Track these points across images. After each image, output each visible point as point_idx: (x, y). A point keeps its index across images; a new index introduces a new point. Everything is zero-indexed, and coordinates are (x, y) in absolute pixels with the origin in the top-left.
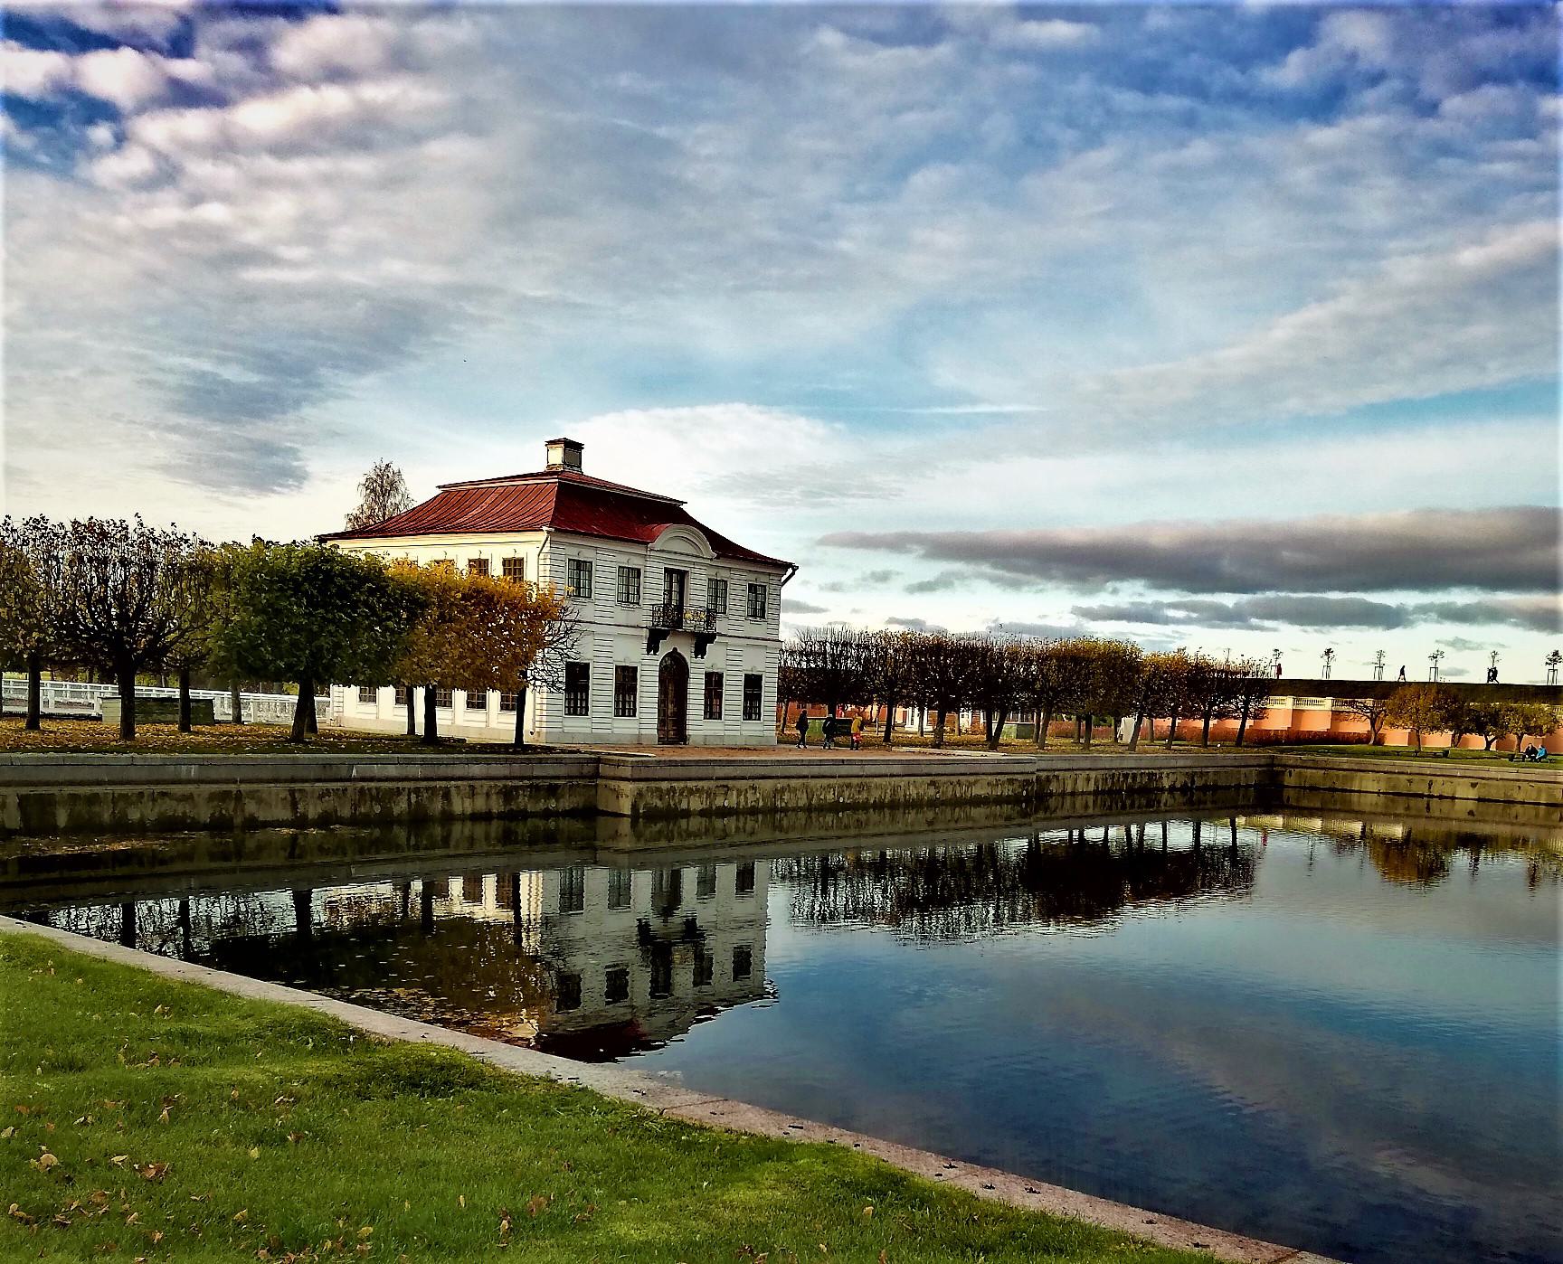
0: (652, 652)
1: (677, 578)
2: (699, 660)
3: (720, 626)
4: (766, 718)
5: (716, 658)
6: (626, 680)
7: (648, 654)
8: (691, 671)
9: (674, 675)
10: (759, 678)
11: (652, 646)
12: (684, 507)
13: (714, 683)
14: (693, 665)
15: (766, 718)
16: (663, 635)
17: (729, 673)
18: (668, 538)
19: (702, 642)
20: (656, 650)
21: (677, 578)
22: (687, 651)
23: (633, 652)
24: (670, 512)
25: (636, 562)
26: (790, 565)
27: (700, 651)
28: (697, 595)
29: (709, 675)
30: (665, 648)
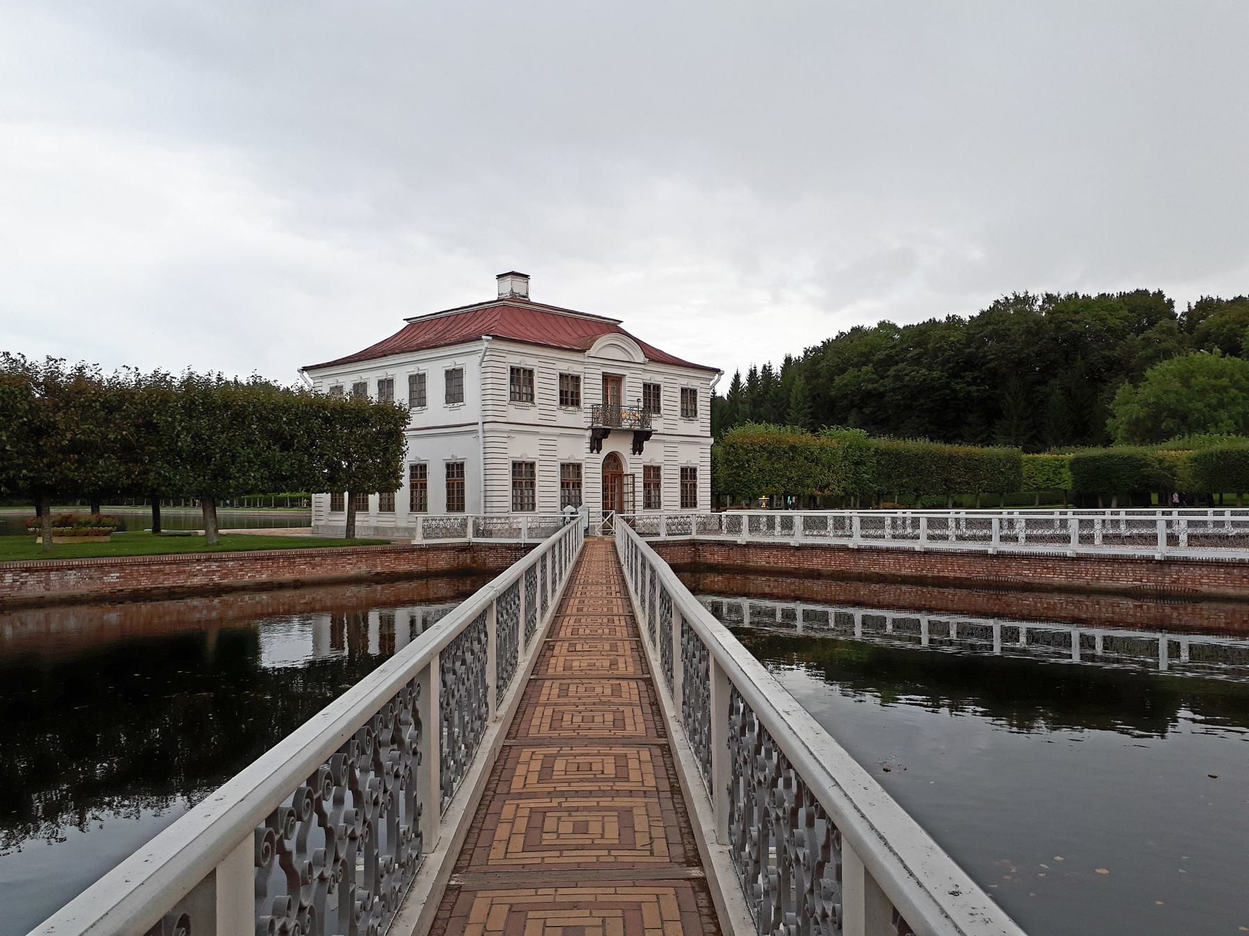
0: (595, 451)
1: (612, 382)
2: (637, 456)
3: (656, 424)
4: (666, 508)
5: (653, 452)
6: (571, 475)
7: (592, 452)
9: (613, 468)
11: (596, 445)
12: (621, 325)
13: (652, 474)
15: (666, 508)
16: (605, 433)
17: (666, 467)
18: (602, 347)
19: (640, 439)
21: (612, 382)
23: (578, 450)
24: (612, 327)
25: (574, 369)
26: (717, 371)
27: (638, 448)
28: (631, 395)
30: (608, 446)
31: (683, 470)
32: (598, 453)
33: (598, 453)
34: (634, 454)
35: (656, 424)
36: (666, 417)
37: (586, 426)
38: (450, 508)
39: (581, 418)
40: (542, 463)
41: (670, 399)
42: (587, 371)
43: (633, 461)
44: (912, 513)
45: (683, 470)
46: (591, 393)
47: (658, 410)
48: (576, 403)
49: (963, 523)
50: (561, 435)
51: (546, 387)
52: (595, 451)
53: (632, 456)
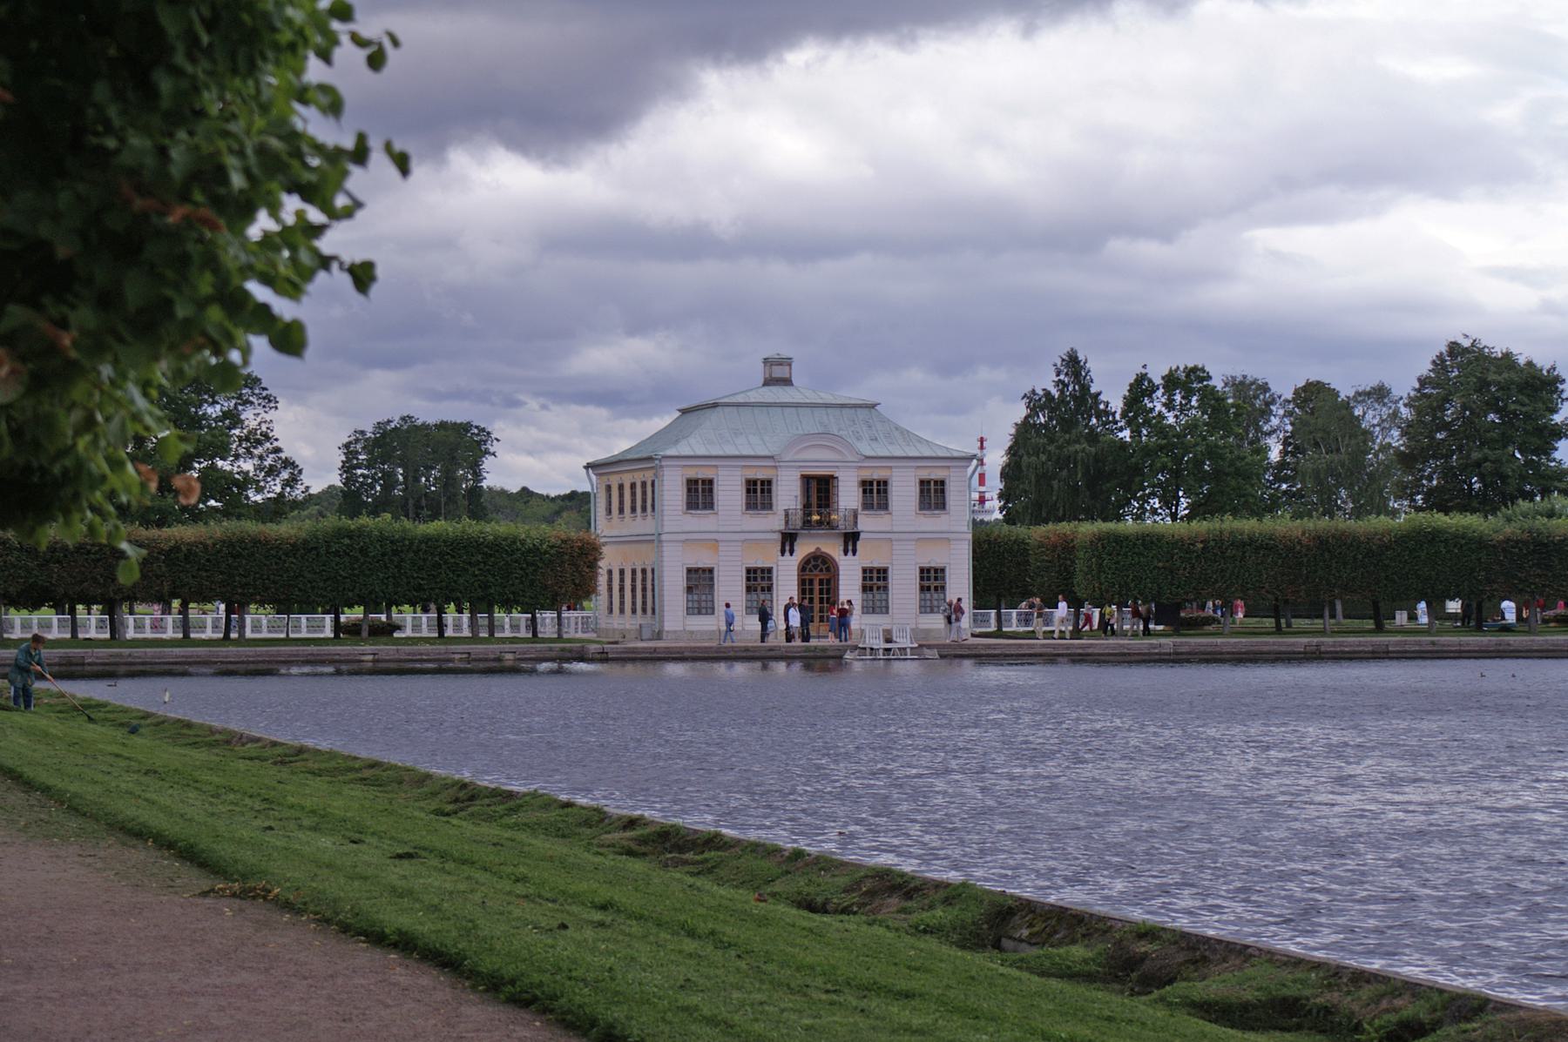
6: (758, 580)
8: (841, 568)
22: (833, 549)
28: (848, 497)
30: (804, 549)
34: (846, 554)
35: (868, 523)
37: (778, 528)
39: (773, 522)
41: (904, 492)
46: (788, 495)
47: (884, 506)
48: (768, 506)
51: (730, 492)
52: (787, 553)
53: (844, 557)
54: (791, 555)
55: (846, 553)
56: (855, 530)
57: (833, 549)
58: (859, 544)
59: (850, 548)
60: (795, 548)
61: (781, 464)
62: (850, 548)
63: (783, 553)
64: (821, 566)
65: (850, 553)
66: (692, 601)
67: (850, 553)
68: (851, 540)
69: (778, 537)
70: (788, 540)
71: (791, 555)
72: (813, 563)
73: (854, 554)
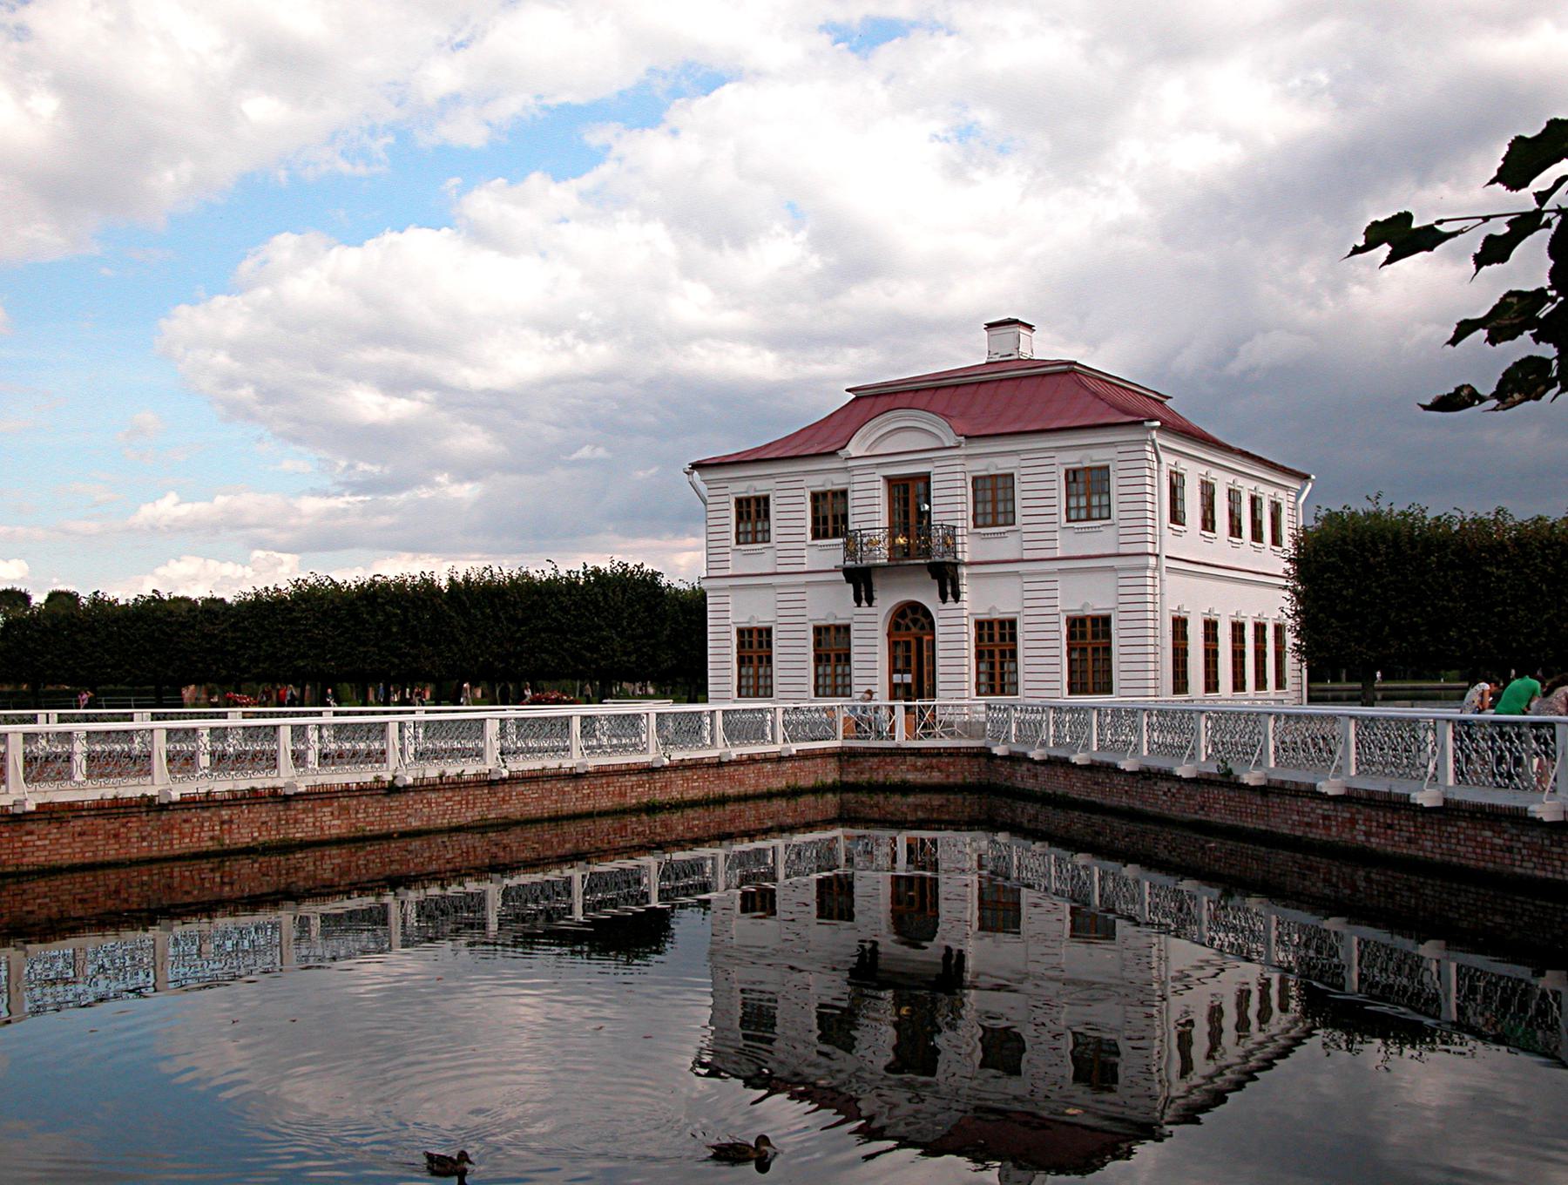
0: (864, 603)
2: (950, 604)
7: (859, 606)
10: (1102, 624)
14: (942, 614)
20: (870, 601)
23: (837, 605)
29: (984, 627)
31: (1076, 625)
32: (870, 605)
33: (870, 605)
34: (944, 600)
36: (1026, 528)
38: (1176, 691)
40: (781, 628)
42: (856, 479)
43: (942, 614)
44: (427, 712)
45: (1076, 625)
49: (511, 729)
50: (808, 584)
52: (864, 603)
54: (870, 605)
55: (944, 600)
56: (947, 559)
57: (928, 597)
58: (965, 588)
59: (949, 590)
60: (875, 595)
61: (851, 463)
62: (949, 590)
63: (858, 600)
64: (907, 621)
65: (950, 598)
66: (748, 677)
67: (950, 598)
68: (946, 577)
69: (841, 576)
70: (861, 580)
71: (870, 605)
72: (910, 615)
73: (957, 598)
